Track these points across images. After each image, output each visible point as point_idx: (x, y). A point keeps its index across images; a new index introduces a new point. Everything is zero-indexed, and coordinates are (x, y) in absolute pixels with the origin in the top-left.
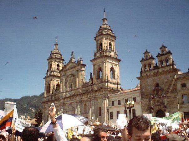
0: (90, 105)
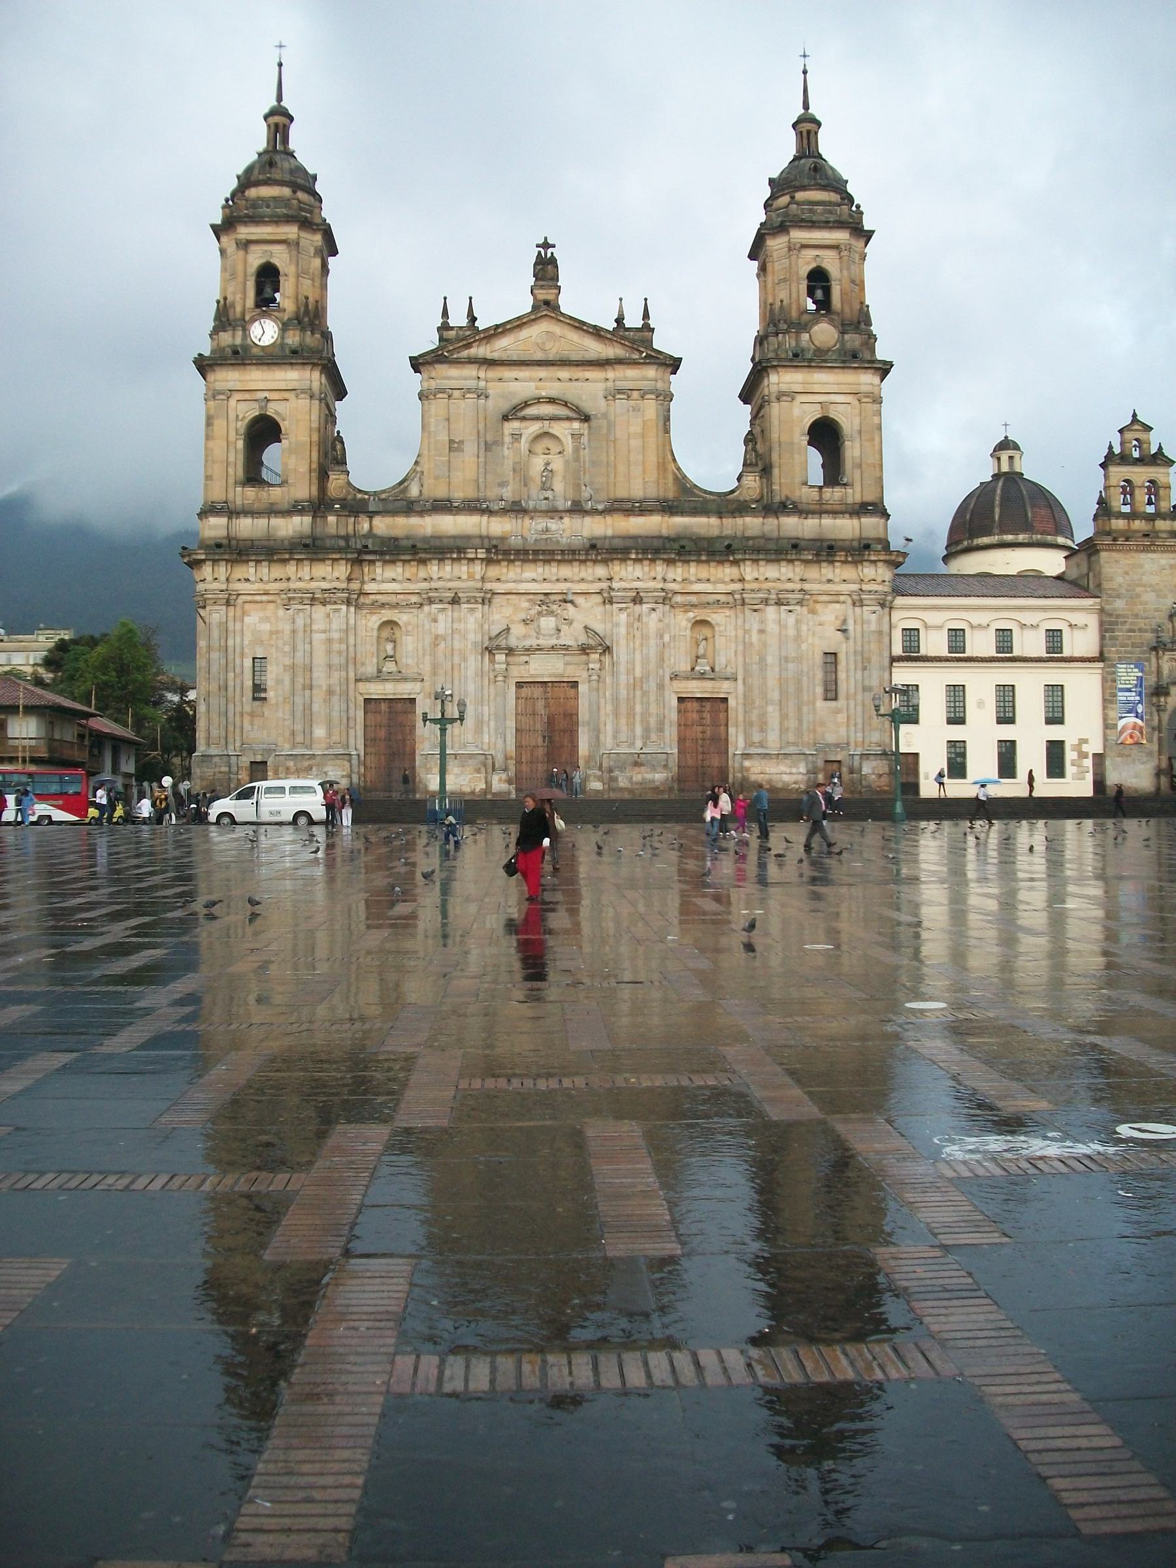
0: (761, 631)
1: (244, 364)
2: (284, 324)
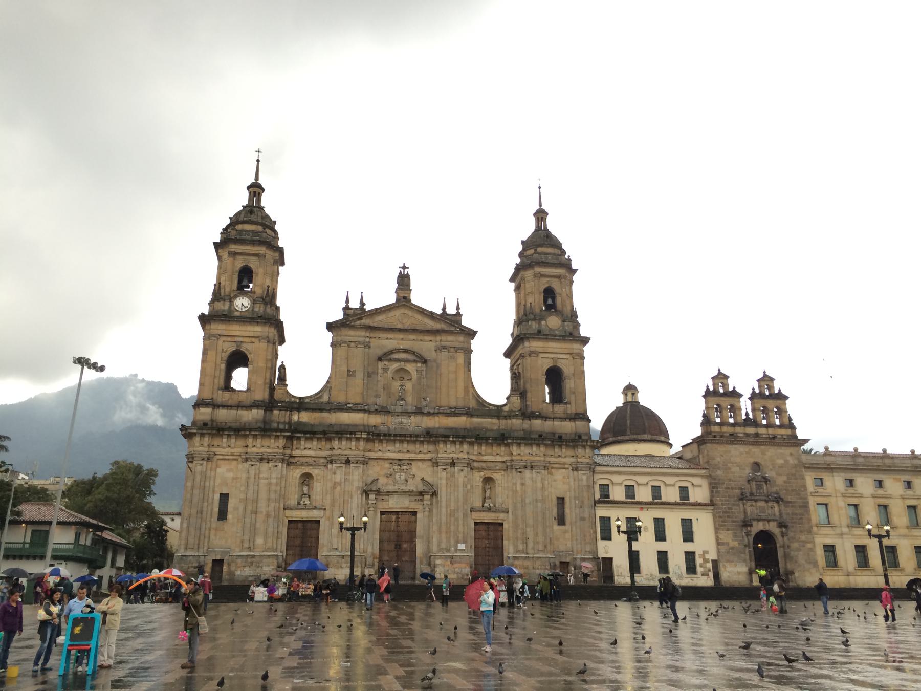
0: (522, 484)
1: (229, 321)
2: (254, 300)
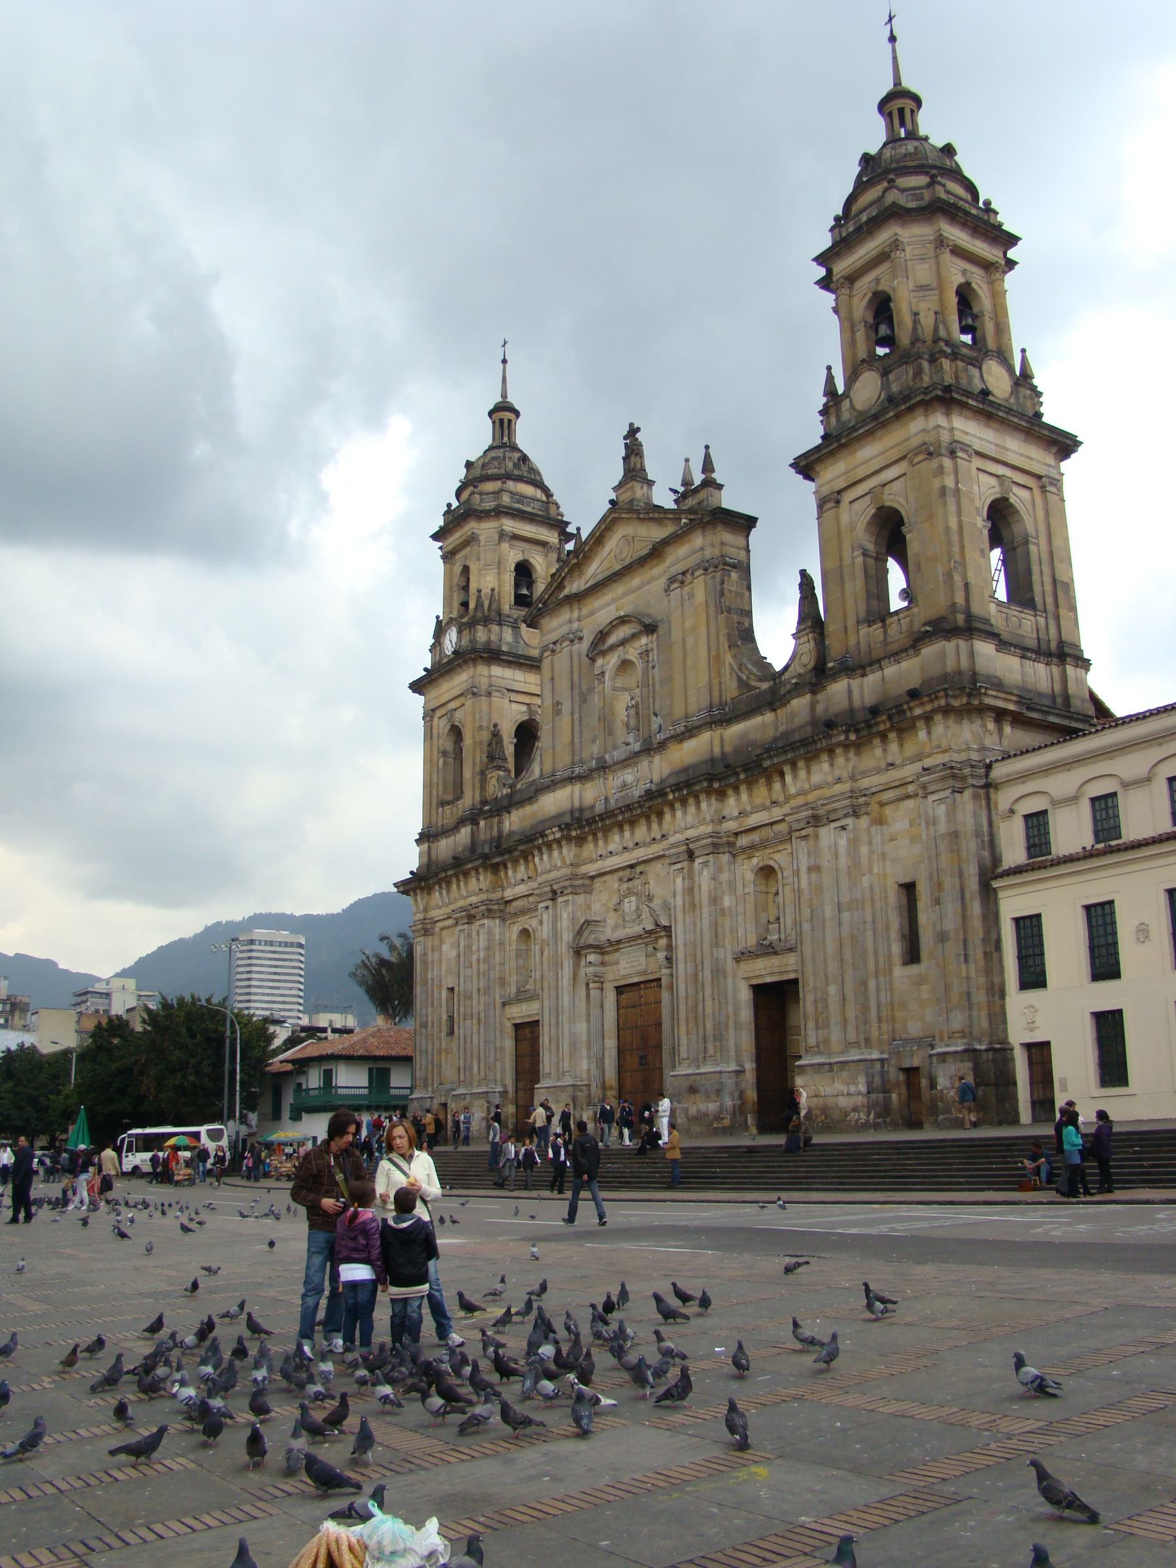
0: (810, 869)
